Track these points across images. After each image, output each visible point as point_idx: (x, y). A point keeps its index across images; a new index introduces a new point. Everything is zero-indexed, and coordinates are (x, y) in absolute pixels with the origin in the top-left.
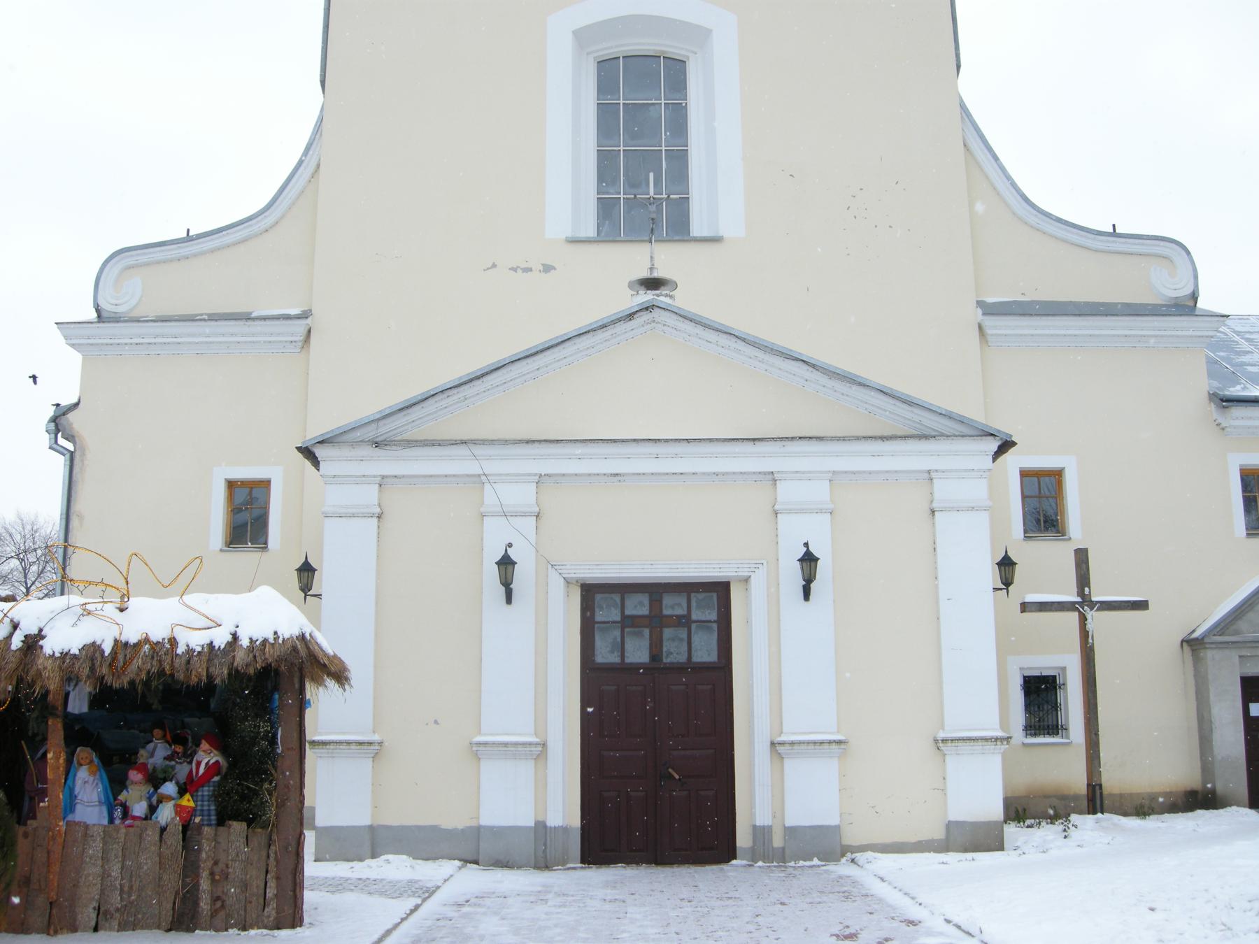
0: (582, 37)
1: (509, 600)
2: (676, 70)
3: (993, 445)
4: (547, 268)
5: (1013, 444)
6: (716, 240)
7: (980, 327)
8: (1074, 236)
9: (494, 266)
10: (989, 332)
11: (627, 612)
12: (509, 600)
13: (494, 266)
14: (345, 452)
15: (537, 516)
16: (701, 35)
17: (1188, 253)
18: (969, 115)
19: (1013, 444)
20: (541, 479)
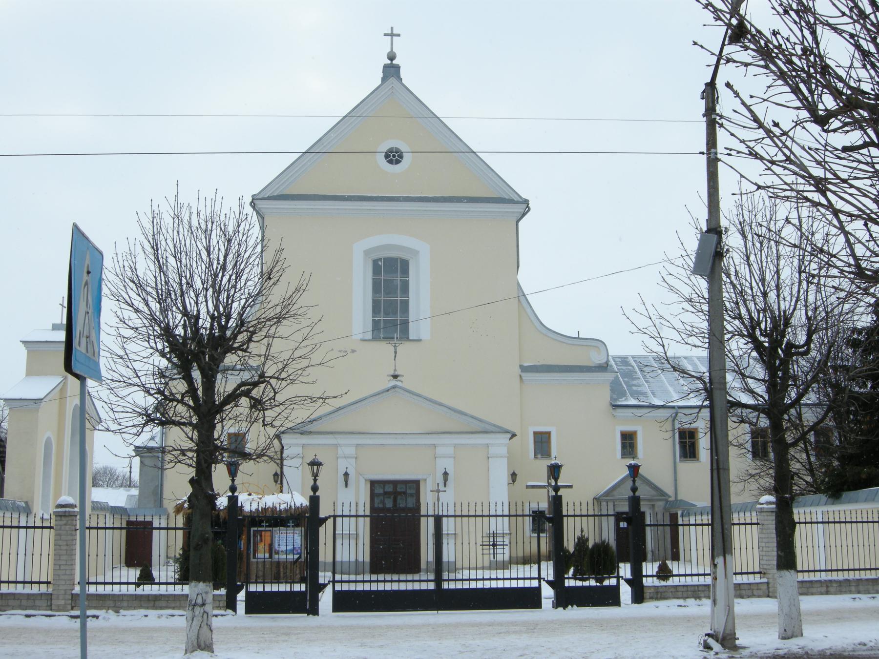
0: (367, 253)
1: (346, 486)
2: (404, 266)
3: (509, 436)
4: (353, 351)
5: (516, 435)
6: (419, 340)
7: (520, 376)
8: (560, 338)
9: (332, 350)
10: (524, 378)
11: (386, 490)
12: (346, 486)
13: (332, 350)
14: (291, 436)
15: (356, 458)
16: (416, 253)
17: (605, 345)
18: (521, 288)
19: (516, 435)
20: (357, 446)
